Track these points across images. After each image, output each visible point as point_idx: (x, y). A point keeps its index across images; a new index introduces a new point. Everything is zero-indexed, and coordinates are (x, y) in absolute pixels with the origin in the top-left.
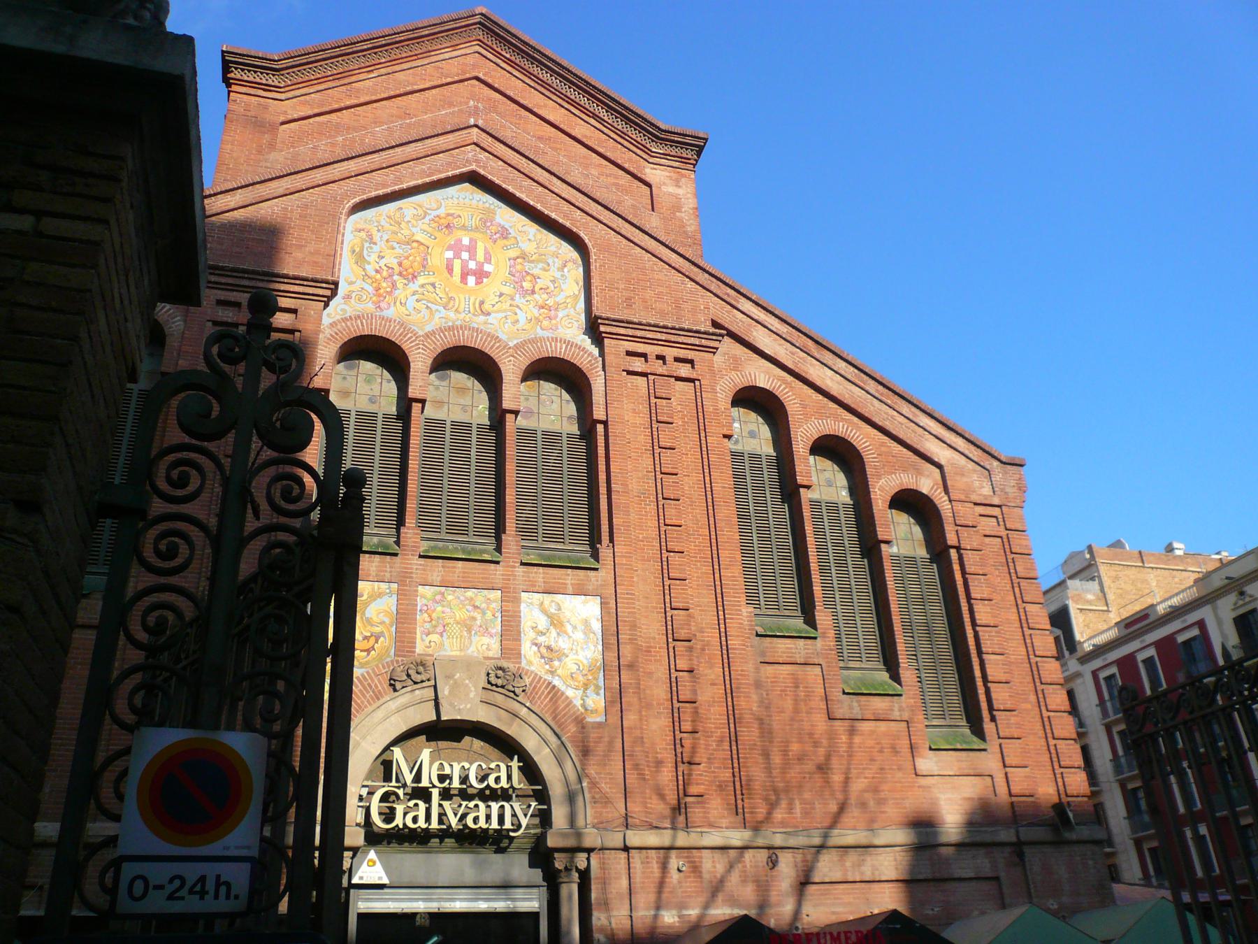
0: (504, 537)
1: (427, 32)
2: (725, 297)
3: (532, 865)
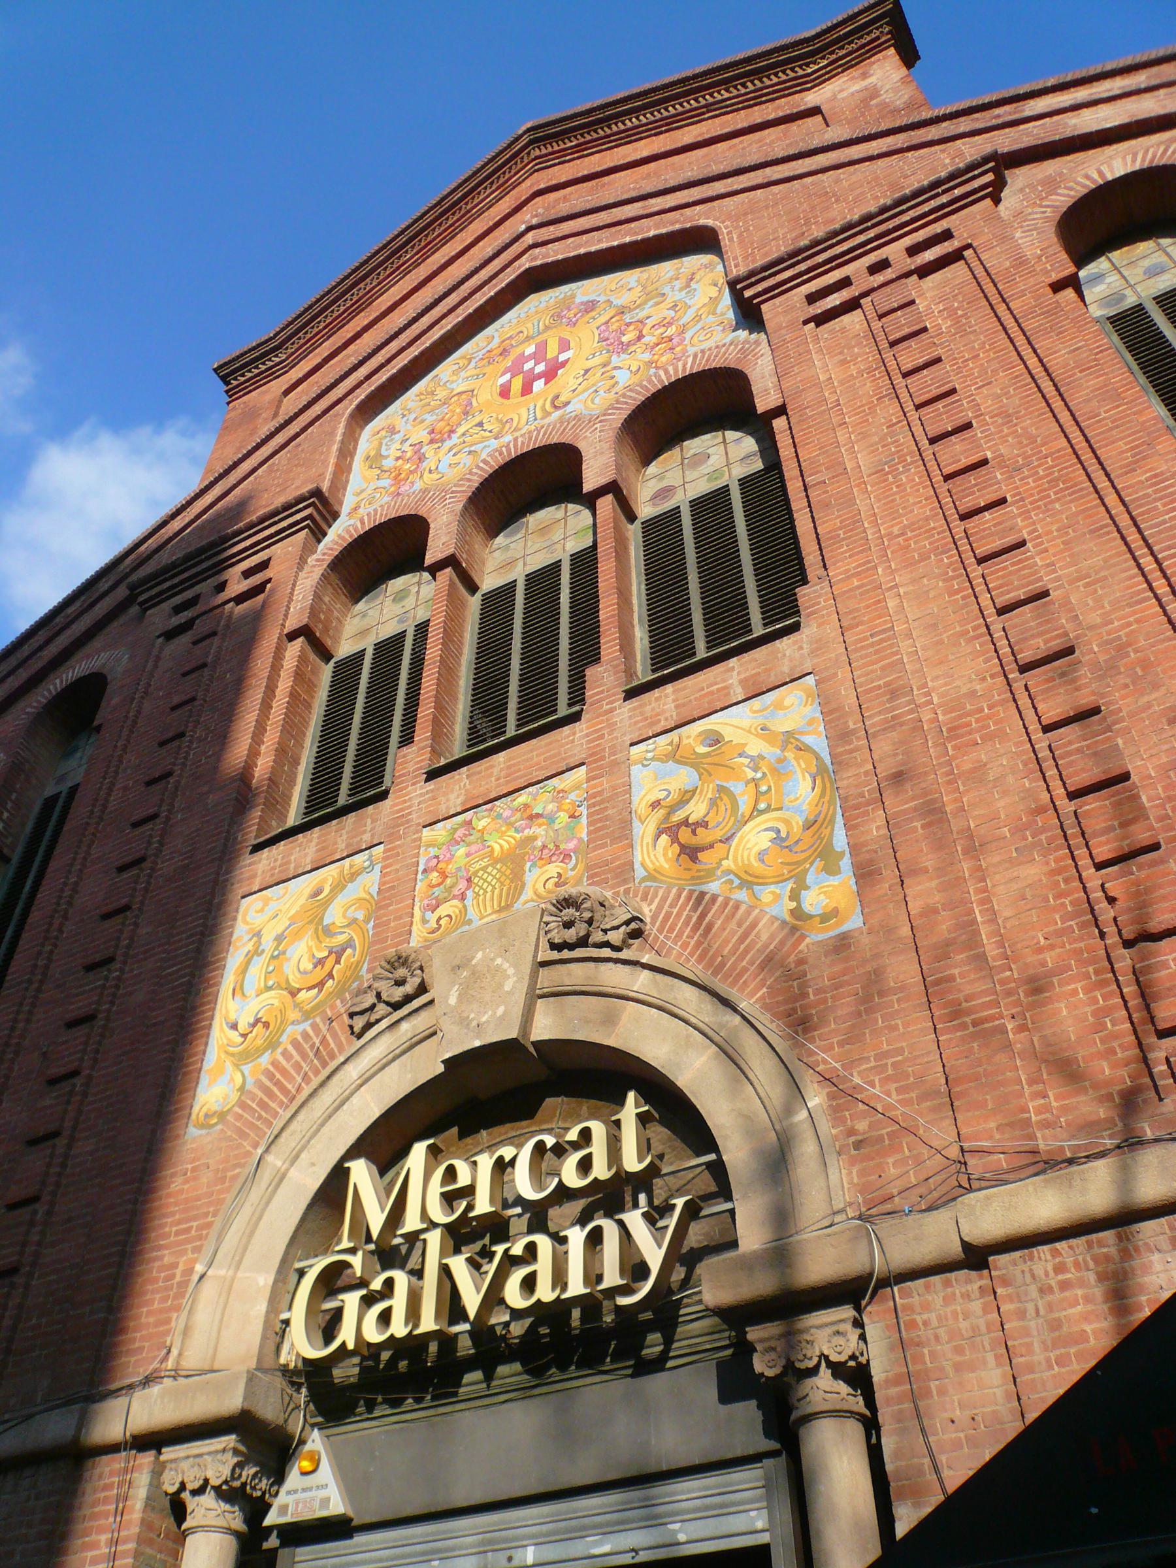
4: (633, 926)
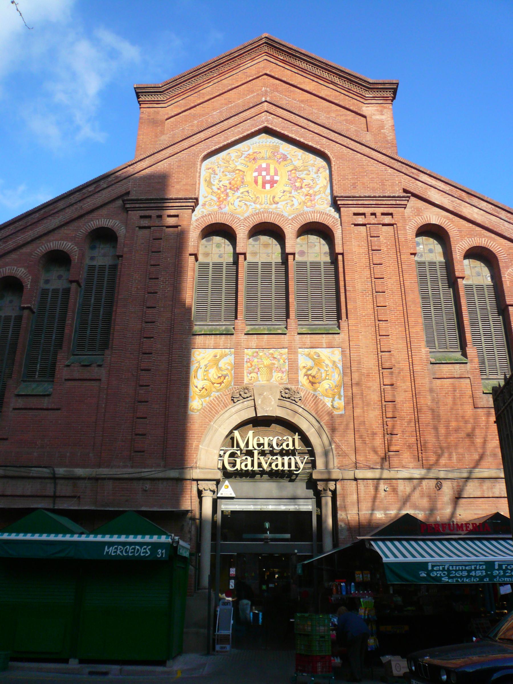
0: (288, 320)
1: (237, 55)
2: (411, 175)
3: (308, 488)
4: (300, 398)
